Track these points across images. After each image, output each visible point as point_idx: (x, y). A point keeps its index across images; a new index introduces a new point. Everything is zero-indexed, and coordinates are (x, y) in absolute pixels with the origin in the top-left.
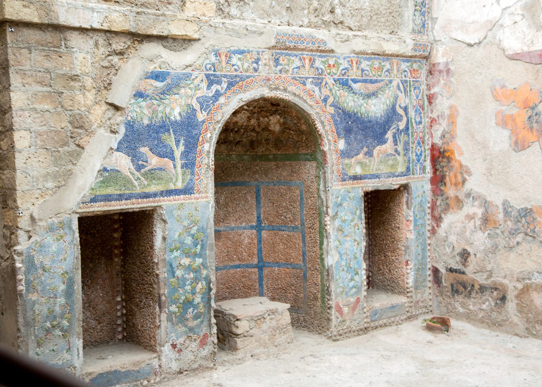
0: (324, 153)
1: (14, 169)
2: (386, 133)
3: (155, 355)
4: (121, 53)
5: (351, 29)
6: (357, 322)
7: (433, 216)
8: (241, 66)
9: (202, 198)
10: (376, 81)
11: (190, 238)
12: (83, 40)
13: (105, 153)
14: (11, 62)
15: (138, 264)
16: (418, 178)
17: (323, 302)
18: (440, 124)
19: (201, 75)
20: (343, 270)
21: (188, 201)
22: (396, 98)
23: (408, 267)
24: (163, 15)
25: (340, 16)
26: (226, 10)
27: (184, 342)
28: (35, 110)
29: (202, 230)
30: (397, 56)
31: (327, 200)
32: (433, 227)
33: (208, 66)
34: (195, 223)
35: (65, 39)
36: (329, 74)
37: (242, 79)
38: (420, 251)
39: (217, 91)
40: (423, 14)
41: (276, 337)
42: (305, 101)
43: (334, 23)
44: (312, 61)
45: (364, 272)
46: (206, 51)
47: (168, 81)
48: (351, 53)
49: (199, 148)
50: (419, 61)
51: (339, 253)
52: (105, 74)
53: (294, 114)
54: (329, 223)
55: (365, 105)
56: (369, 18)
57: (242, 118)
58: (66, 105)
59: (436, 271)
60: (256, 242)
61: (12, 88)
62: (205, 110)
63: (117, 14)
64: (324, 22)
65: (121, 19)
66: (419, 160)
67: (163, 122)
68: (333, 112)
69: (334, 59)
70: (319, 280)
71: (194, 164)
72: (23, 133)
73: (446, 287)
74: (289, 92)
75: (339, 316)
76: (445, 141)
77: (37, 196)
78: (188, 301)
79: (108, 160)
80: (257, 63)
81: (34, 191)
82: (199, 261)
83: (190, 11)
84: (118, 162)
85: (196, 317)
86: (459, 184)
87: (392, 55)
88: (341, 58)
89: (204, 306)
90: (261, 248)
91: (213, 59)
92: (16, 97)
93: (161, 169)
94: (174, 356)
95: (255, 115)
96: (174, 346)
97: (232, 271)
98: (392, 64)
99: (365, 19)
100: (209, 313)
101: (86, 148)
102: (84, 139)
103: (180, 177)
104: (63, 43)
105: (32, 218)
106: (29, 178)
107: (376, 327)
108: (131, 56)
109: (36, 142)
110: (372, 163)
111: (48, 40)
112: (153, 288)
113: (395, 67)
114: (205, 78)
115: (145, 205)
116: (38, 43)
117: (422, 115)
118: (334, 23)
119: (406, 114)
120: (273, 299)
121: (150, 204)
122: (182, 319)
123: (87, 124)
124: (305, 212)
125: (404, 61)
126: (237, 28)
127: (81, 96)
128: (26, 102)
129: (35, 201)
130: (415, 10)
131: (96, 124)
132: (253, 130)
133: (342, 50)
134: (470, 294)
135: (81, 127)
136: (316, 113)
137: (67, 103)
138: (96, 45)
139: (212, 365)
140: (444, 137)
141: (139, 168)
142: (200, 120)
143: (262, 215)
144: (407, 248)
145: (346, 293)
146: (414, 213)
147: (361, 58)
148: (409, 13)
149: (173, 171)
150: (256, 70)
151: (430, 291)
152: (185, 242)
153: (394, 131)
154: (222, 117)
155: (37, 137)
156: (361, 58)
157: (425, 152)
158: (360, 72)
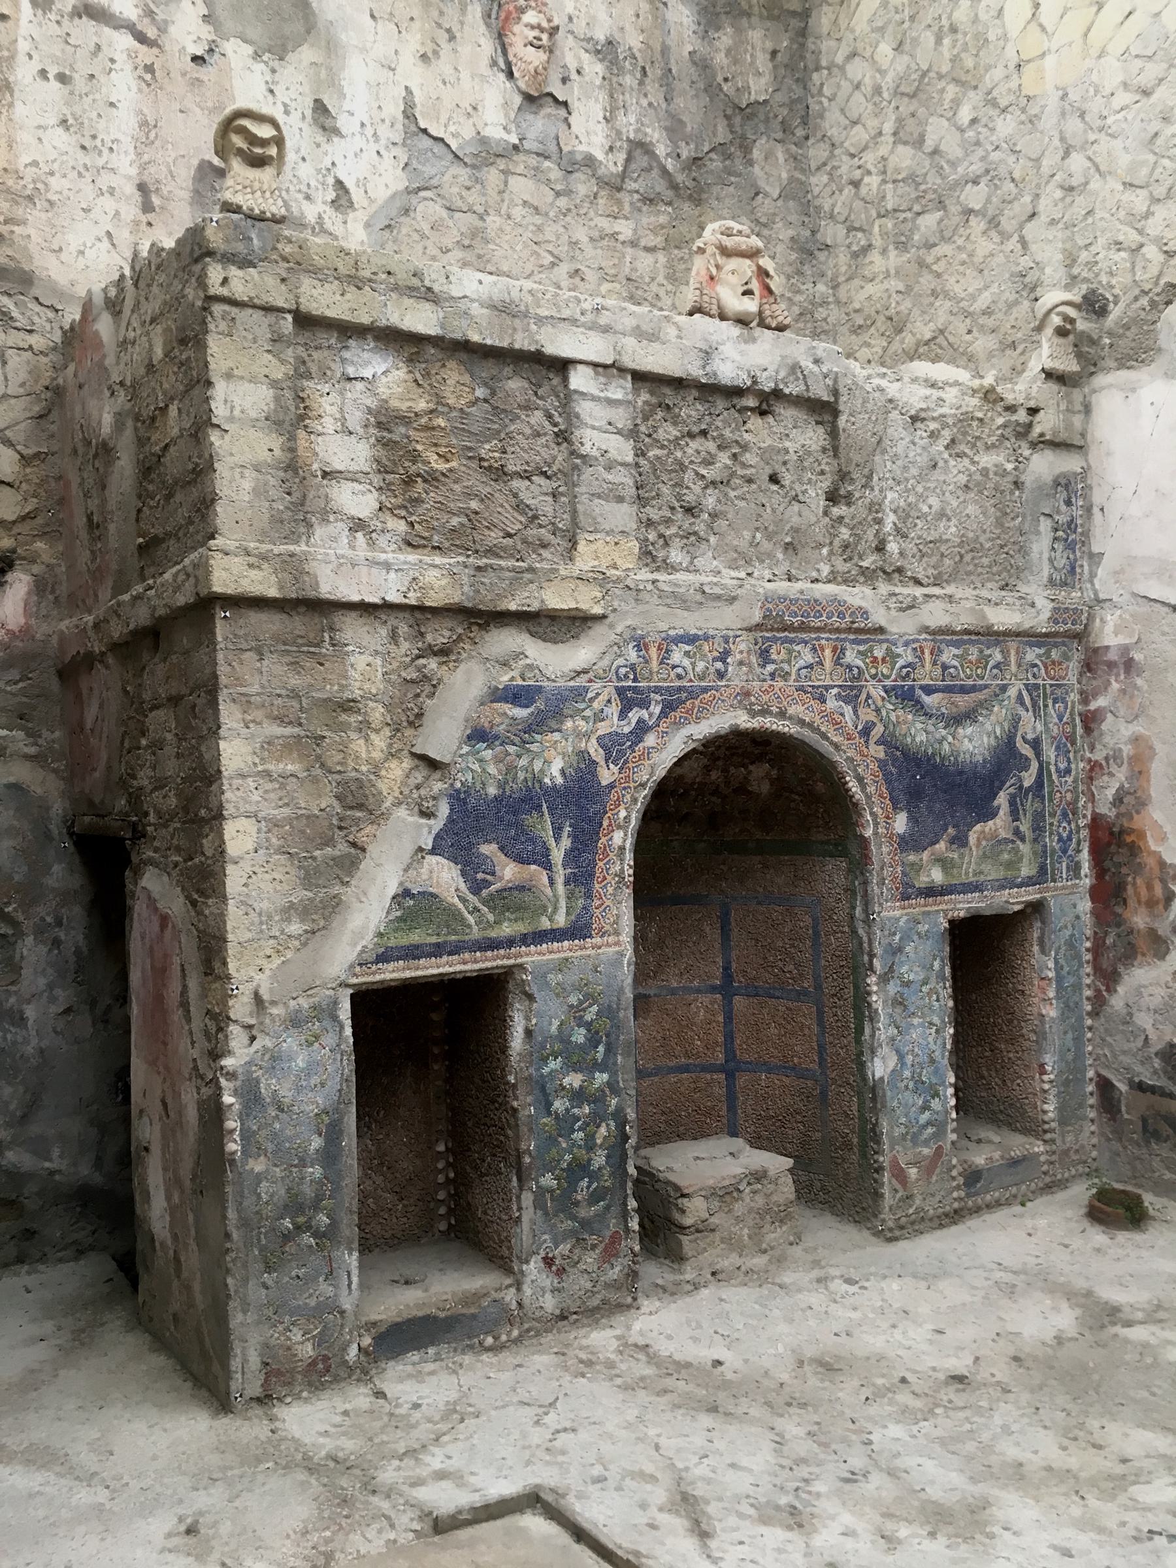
0: (864, 843)
1: (224, 898)
2: (995, 795)
3: (508, 1281)
5: (921, 584)
6: (938, 1198)
7: (1098, 969)
8: (689, 668)
9: (608, 945)
10: (973, 689)
11: (583, 1031)
12: (366, 628)
13: (406, 859)
14: (223, 680)
15: (477, 1080)
16: (1063, 888)
17: (864, 1155)
18: (1111, 775)
19: (606, 691)
20: (907, 1087)
21: (579, 953)
22: (1016, 721)
23: (1045, 1078)
24: (531, 570)
25: (896, 556)
26: (661, 554)
28: (267, 774)
29: (608, 1012)
30: (1018, 634)
31: (870, 940)
32: (1098, 991)
33: (623, 671)
34: (591, 998)
35: (332, 629)
36: (874, 677)
37: (692, 694)
38: (1069, 1042)
39: (640, 721)
40: (1070, 546)
41: (764, 1230)
42: (824, 736)
43: (885, 572)
44: (838, 653)
45: (951, 1091)
46: (618, 639)
47: (540, 704)
48: (920, 632)
49: (603, 840)
50: (1064, 644)
51: (898, 1051)
52: (410, 695)
53: (800, 761)
54: (875, 988)
55: (950, 739)
56: (957, 558)
57: (692, 772)
58: (329, 764)
59: (1105, 1086)
60: (721, 1019)
61: (222, 732)
62: (615, 763)
63: (436, 573)
64: (863, 571)
65: (443, 582)
66: (1065, 851)
67: (528, 789)
68: (882, 755)
69: (885, 646)
70: (855, 1108)
73: (1130, 1122)
74: (790, 718)
75: (898, 1186)
76: (1123, 809)
77: (269, 952)
78: (579, 1165)
79: (412, 873)
81: (262, 942)
82: (601, 1078)
84: (435, 875)
85: (594, 1198)
86: (1157, 903)
87: (1008, 634)
88: (900, 644)
89: (612, 1174)
90: (732, 1031)
91: (632, 655)
92: (230, 751)
93: (521, 888)
94: (548, 1283)
95: (720, 763)
96: (548, 1261)
97: (673, 1078)
98: (1005, 653)
99: (947, 562)
101: (369, 848)
102: (367, 830)
103: (563, 903)
104: (326, 635)
105: (257, 998)
106: (253, 915)
108: (464, 655)
109: (268, 840)
110: (966, 859)
111: (297, 632)
112: (507, 1137)
113: (1013, 659)
114: (615, 696)
115: (489, 964)
116: (277, 638)
117: (1071, 755)
118: (885, 572)
119: (1038, 754)
120: (757, 1142)
121: (500, 962)
122: (564, 1202)
123: (371, 800)
124: (823, 962)
125: (1031, 645)
126: (682, 590)
127: (362, 742)
128: (249, 759)
129: (264, 962)
130: (1055, 539)
131: (390, 798)
132: (716, 792)
133: (901, 626)
135: (360, 806)
136: (850, 760)
138: (394, 636)
139: (629, 1300)
140: (1121, 802)
142: (604, 783)
143: (734, 965)
144: (1042, 1035)
145: (915, 1137)
146: (1056, 962)
147: (942, 641)
148: (1041, 546)
149: (548, 891)
150: (721, 675)
151: (1093, 1128)
152: (573, 1039)
153: (1012, 790)
154: (651, 774)
155: (269, 831)
156: (942, 641)
157: (1078, 832)
158: (940, 671)
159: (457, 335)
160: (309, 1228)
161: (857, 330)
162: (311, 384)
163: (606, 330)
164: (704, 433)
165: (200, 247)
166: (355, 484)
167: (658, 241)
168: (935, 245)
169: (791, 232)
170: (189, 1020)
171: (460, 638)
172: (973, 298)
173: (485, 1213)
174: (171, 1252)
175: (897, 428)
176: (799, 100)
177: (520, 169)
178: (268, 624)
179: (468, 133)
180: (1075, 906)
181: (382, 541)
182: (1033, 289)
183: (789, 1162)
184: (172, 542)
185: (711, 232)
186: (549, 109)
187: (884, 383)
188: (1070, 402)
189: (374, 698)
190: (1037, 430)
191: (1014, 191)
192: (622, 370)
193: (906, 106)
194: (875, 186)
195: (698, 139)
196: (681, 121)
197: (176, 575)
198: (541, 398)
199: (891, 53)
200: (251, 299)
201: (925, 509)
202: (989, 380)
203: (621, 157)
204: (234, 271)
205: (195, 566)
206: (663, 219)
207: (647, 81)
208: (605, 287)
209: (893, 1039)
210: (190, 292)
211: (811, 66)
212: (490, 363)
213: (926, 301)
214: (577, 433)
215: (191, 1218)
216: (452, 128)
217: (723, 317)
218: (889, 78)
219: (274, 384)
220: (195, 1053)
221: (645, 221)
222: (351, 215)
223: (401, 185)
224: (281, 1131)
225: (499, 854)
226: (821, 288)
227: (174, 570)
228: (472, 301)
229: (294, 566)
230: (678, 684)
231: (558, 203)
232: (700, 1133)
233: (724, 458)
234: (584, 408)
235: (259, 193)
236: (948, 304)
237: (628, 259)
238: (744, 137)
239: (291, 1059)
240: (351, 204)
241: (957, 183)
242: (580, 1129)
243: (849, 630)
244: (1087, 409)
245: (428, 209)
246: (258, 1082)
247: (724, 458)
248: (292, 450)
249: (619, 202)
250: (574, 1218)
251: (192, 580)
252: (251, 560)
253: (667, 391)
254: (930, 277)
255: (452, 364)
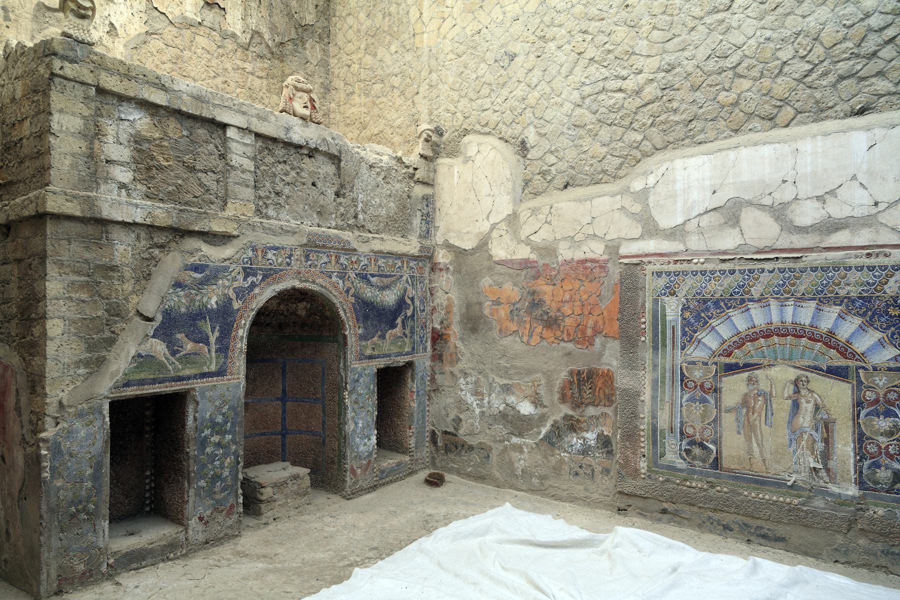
0: (345, 337)
3: (181, 529)
4: (162, 247)
9: (234, 379)
10: (390, 276)
11: (221, 417)
14: (49, 253)
16: (421, 356)
17: (340, 466)
19: (238, 268)
22: (405, 290)
24: (205, 213)
26: (264, 211)
27: (211, 514)
28: (71, 298)
30: (407, 256)
33: (246, 260)
34: (224, 402)
35: (107, 232)
36: (351, 269)
37: (276, 272)
38: (420, 417)
40: (428, 223)
44: (338, 258)
45: (375, 437)
47: (207, 272)
49: (234, 333)
52: (145, 265)
59: (433, 433)
60: (280, 412)
61: (47, 277)
63: (159, 210)
64: (349, 225)
65: (164, 215)
68: (353, 301)
71: (228, 348)
72: (57, 321)
74: (317, 284)
75: (353, 477)
80: (290, 258)
82: (229, 437)
83: (230, 212)
85: (224, 489)
91: (250, 254)
93: (195, 354)
96: (201, 519)
97: (257, 438)
98: (403, 262)
99: (381, 224)
100: (236, 484)
103: (214, 360)
104: (104, 235)
105: (60, 403)
107: (384, 484)
109: (69, 329)
112: (183, 465)
115: (178, 388)
116: (79, 235)
120: (294, 464)
121: (183, 387)
122: (211, 493)
123: (124, 312)
133: (363, 249)
134: (460, 452)
135: (118, 315)
136: (341, 302)
137: (105, 292)
138: (138, 238)
139: (237, 533)
141: (174, 353)
142: (235, 308)
144: (412, 415)
148: (417, 221)
150: (288, 264)
153: (403, 317)
155: (70, 325)
159: (176, 107)
160: (85, 510)
161: (347, 125)
162: (103, 120)
163: (244, 113)
164: (285, 162)
165: (49, 50)
166: (122, 167)
167: (264, 74)
168: (379, 97)
169: (321, 80)
170: (20, 415)
171: (169, 242)
172: (394, 120)
173: (170, 501)
174: (4, 530)
175: (364, 169)
176: (326, 27)
177: (201, 33)
178: (75, 228)
179: (177, 13)
180: (424, 363)
181: (134, 194)
182: (416, 122)
183: (308, 471)
184: (21, 185)
185: (290, 80)
186: (217, 10)
187: (359, 150)
188: (429, 167)
189: (127, 265)
190: (417, 176)
191: (411, 82)
192: (250, 131)
193: (371, 40)
194: (356, 69)
195: (283, 35)
196: (276, 27)
197: (24, 200)
198: (213, 139)
199: (364, 17)
200: (75, 78)
201: (374, 203)
202: (399, 154)
203: (249, 36)
204: (66, 64)
205: (37, 198)
206: (266, 66)
207: (262, 6)
208: (238, 90)
209: (353, 417)
210: (42, 70)
211: (332, 15)
212: (190, 121)
213: (376, 118)
214: (229, 155)
215: (18, 511)
216: (170, 10)
217: (295, 115)
218: (364, 27)
219: (84, 118)
220: (24, 431)
221: (258, 65)
222: (117, 40)
223: (144, 31)
224: (71, 466)
225: (186, 338)
226: (333, 105)
227: (23, 198)
228: (183, 93)
229: (90, 202)
230: (270, 267)
231: (218, 50)
232: (269, 461)
233: (293, 173)
234: (233, 145)
235: (81, 31)
236: (384, 121)
237: (250, 80)
238: (302, 38)
239: (77, 432)
240: (117, 35)
241: (389, 74)
242: (218, 460)
243: (342, 249)
244: (435, 171)
245: (155, 44)
246: (60, 443)
247: (293, 173)
248: (91, 149)
249: (247, 55)
250: (214, 499)
251: (34, 204)
252: (68, 197)
253: (270, 143)
254: (378, 109)
255: (172, 119)
